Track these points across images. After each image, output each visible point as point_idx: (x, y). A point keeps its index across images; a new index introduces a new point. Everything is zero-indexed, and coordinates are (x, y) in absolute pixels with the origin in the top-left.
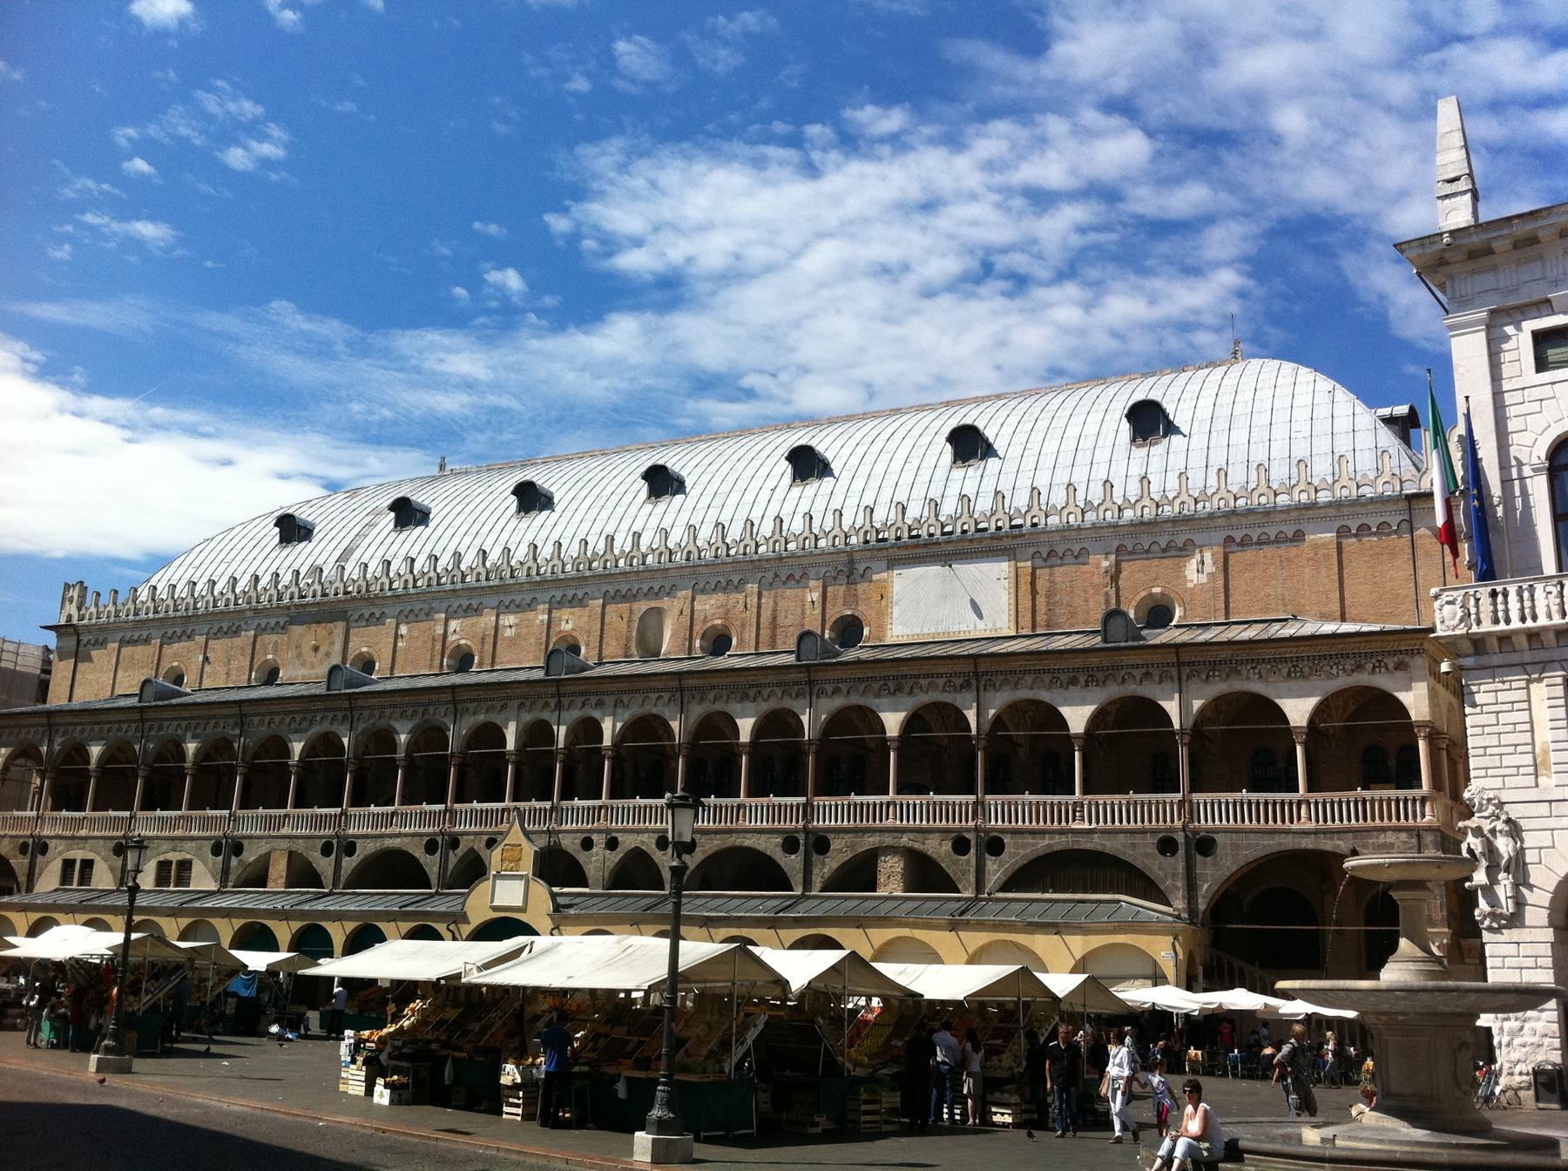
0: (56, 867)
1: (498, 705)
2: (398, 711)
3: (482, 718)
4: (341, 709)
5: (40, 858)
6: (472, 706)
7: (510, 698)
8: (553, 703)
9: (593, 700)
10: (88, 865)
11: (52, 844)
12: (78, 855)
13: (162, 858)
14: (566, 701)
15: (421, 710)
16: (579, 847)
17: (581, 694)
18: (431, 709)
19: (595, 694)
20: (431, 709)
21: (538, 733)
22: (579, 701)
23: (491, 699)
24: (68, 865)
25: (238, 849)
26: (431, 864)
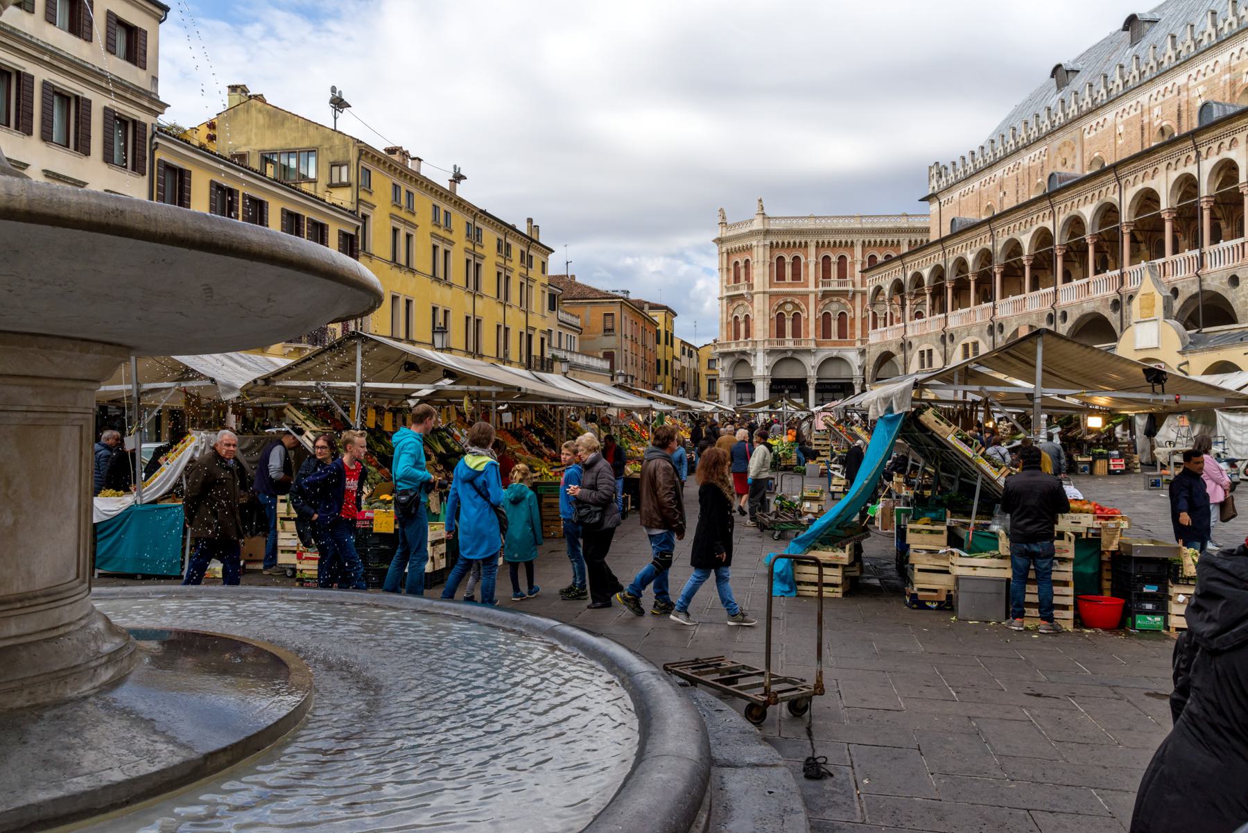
0: (916, 357)
1: (1150, 171)
2: (1083, 198)
3: (1140, 186)
4: (1046, 208)
5: (909, 353)
6: (1131, 178)
7: (1159, 162)
8: (1193, 154)
9: (1227, 141)
10: (930, 351)
11: (915, 342)
12: (925, 347)
13: (964, 342)
14: (1203, 150)
15: (1097, 193)
16: (1227, 287)
17: (1216, 139)
18: (1104, 189)
19: (1227, 135)
20: (1104, 189)
21: (1188, 185)
22: (1215, 146)
23: (1146, 167)
24: (922, 353)
25: (1001, 327)
26: (1113, 318)
